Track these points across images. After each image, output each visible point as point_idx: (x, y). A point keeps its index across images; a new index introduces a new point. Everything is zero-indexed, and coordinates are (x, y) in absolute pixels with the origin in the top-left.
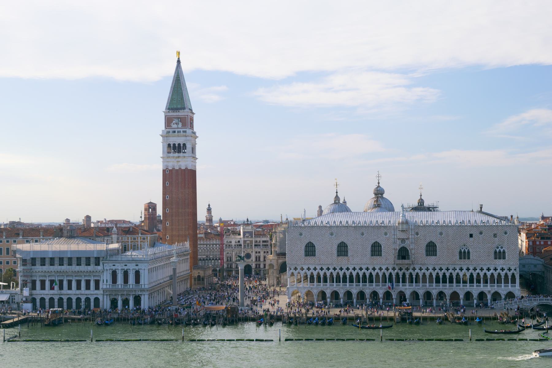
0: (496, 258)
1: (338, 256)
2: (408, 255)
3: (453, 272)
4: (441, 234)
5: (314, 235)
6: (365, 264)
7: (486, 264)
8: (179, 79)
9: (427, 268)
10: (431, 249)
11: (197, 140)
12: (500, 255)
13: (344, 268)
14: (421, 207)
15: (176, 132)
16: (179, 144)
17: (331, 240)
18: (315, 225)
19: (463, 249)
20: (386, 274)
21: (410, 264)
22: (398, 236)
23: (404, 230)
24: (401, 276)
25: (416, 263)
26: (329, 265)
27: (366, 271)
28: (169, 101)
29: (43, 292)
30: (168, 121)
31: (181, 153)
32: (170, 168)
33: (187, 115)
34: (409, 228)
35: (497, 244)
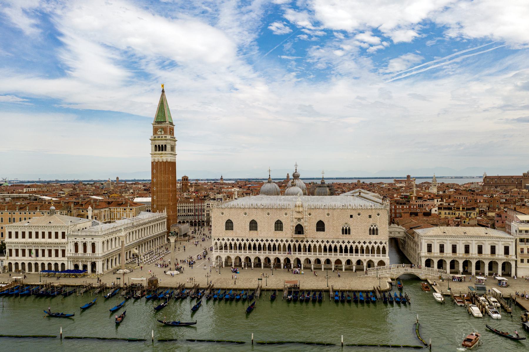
0: (370, 234)
1: (250, 230)
2: (303, 231)
3: (337, 244)
4: (328, 214)
6: (270, 237)
9: (317, 240)
10: (320, 227)
12: (374, 232)
13: (255, 239)
16: (162, 145)
18: (233, 207)
21: (304, 238)
24: (297, 247)
26: (244, 237)
29: (24, 258)
30: (155, 130)
32: (156, 161)
34: (304, 210)
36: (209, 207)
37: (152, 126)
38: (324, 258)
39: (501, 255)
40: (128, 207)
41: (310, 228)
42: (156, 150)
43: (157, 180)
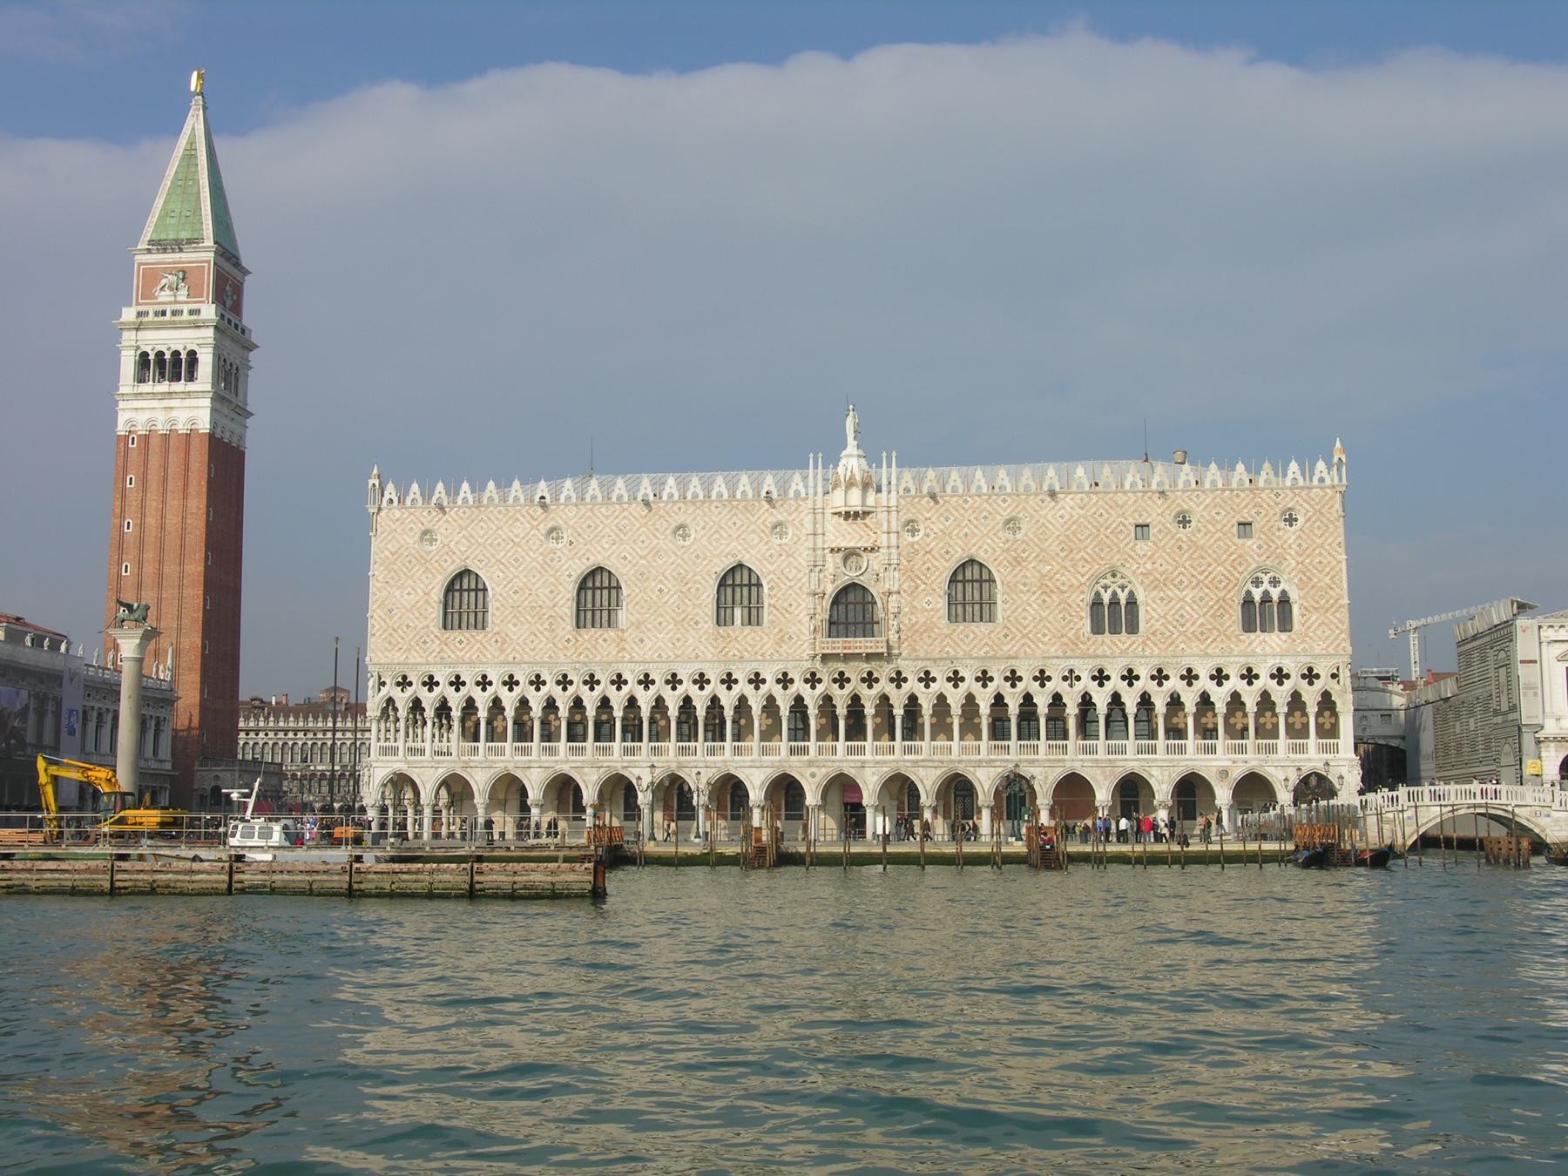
0: (1248, 627)
4: (1011, 523)
5: (480, 541)
6: (689, 661)
7: (1209, 651)
8: (193, 152)
11: (253, 356)
15: (168, 313)
16: (176, 354)
17: (552, 560)
19: (1110, 591)
20: (779, 702)
21: (879, 656)
22: (829, 536)
23: (856, 514)
25: (903, 654)
31: (179, 380)
33: (202, 262)
35: (1254, 566)
43: (142, 526)
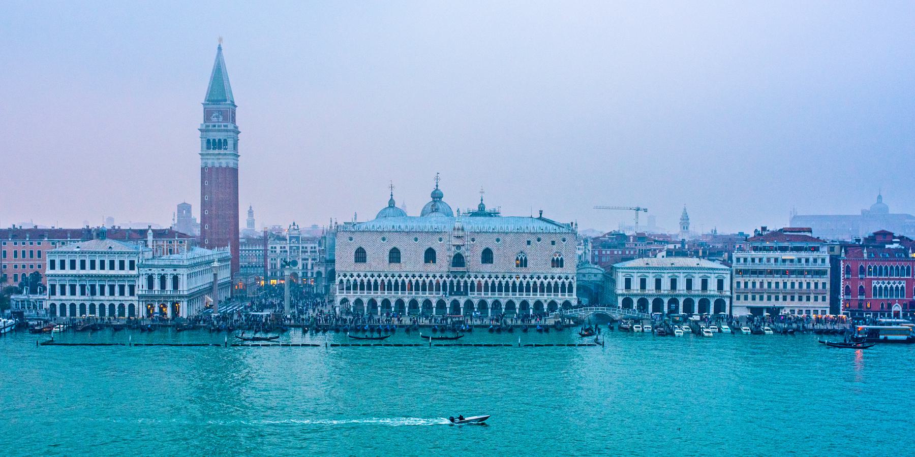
0: (553, 267)
9: (483, 276)
10: (487, 256)
12: (558, 263)
13: (397, 275)
14: (481, 212)
16: (220, 140)
18: (366, 230)
27: (419, 279)
28: (209, 92)
30: (208, 115)
32: (210, 165)
36: (275, 252)
37: (202, 108)
38: (491, 300)
39: (714, 291)
40: (176, 238)
41: (473, 259)
42: (208, 148)
